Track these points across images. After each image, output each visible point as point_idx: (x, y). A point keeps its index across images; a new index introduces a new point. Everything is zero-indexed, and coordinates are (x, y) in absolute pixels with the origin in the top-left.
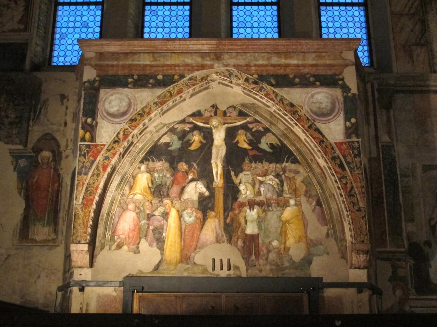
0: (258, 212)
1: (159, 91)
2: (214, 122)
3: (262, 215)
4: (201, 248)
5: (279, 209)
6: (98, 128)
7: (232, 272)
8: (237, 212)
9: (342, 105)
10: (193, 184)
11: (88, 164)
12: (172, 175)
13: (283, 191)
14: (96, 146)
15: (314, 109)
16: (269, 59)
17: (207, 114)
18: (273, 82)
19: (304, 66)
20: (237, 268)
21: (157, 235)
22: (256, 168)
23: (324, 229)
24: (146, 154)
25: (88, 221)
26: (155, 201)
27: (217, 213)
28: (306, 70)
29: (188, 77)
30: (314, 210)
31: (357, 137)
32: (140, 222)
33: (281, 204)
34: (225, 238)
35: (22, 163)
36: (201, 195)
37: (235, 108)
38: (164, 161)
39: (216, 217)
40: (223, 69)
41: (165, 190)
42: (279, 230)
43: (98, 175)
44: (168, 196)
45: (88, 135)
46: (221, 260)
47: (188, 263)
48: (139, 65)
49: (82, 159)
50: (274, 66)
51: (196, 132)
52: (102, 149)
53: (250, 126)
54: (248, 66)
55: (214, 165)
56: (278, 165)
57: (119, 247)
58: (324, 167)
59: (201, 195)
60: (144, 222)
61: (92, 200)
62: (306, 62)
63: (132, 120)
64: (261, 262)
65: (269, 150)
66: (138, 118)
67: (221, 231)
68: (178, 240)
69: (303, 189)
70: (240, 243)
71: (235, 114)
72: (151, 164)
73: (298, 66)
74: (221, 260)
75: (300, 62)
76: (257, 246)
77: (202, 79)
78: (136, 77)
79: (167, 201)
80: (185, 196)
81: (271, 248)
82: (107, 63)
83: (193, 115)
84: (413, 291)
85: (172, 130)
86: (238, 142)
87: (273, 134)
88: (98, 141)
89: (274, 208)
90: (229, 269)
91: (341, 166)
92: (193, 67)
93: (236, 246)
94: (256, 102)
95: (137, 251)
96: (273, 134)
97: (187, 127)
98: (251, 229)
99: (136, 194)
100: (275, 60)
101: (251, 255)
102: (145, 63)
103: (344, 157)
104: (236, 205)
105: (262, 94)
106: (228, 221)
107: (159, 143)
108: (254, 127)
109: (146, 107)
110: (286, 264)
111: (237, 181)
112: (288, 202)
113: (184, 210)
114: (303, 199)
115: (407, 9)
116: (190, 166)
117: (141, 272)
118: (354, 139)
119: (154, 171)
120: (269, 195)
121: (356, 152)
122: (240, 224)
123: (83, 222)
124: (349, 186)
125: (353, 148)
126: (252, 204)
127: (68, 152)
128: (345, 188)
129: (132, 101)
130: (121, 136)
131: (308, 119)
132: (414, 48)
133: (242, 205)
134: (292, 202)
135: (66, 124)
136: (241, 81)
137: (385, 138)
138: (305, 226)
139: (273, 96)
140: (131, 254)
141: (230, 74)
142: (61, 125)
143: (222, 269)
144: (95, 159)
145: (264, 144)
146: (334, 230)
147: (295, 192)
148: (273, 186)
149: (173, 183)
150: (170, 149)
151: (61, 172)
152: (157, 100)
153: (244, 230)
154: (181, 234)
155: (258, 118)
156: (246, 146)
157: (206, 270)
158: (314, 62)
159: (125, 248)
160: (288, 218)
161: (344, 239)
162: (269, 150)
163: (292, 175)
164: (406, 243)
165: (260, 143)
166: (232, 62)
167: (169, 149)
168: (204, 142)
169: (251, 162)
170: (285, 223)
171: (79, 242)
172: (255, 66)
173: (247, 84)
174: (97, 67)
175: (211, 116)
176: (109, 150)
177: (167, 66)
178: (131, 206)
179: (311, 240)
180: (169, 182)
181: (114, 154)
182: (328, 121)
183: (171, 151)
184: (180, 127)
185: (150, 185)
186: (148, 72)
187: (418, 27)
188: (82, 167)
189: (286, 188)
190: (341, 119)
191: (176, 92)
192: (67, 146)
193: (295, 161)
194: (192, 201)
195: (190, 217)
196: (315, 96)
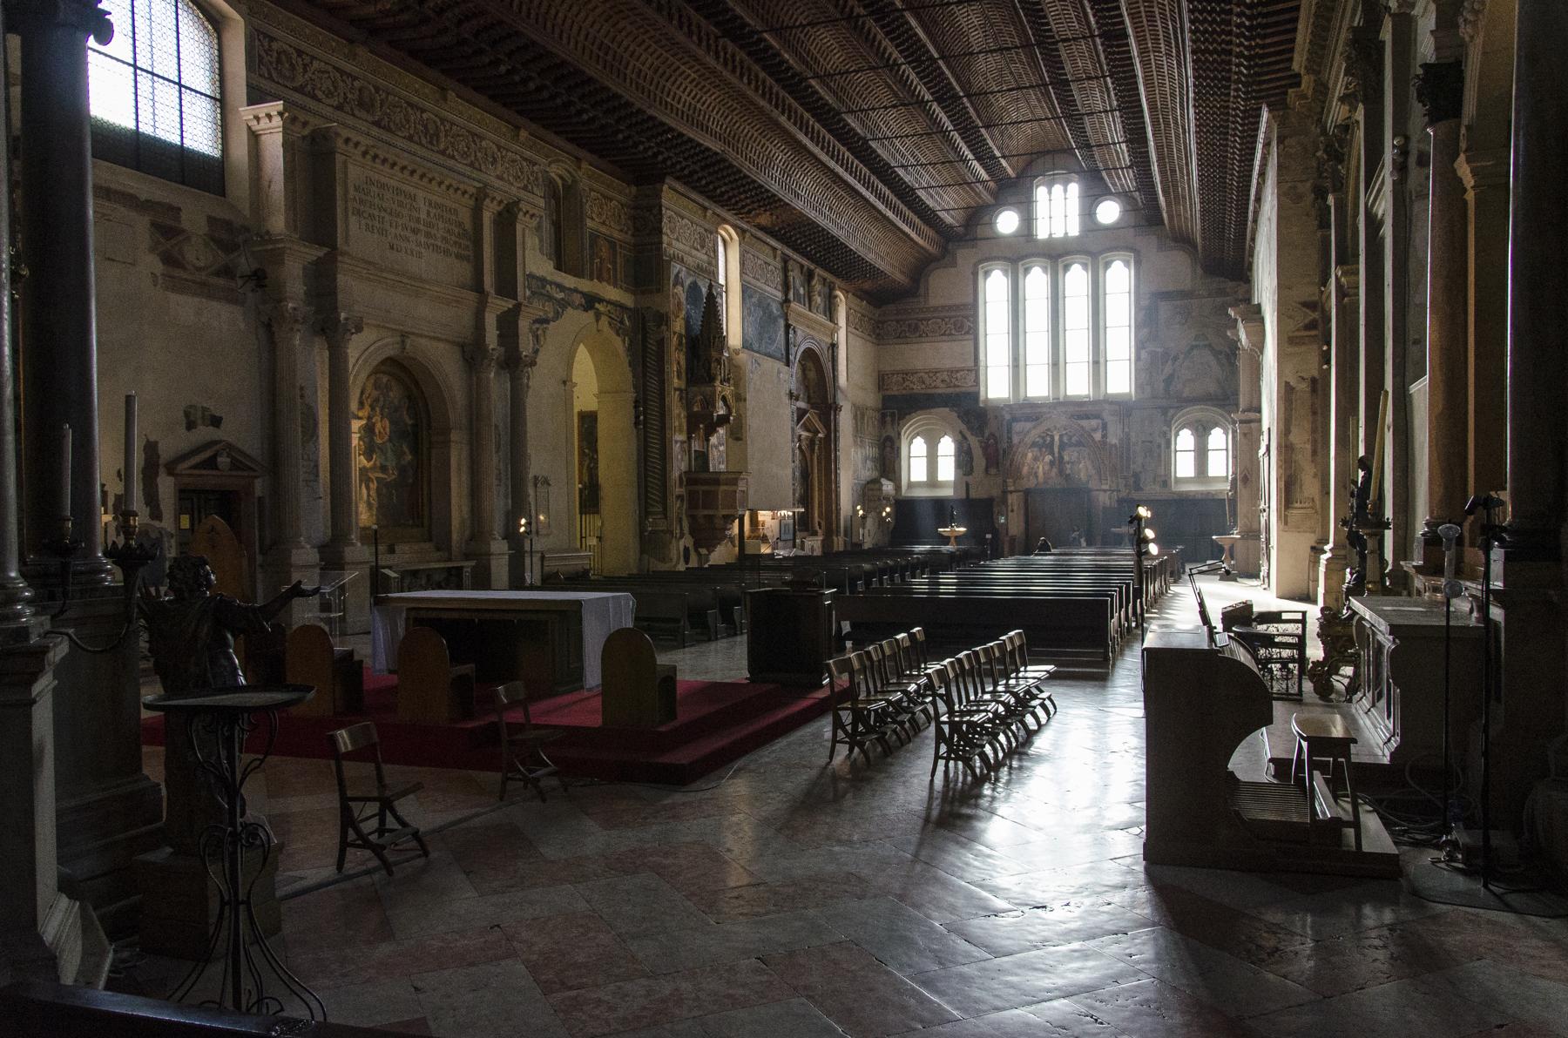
98: (1068, 472)
137: (1126, 430)
154: (1044, 474)
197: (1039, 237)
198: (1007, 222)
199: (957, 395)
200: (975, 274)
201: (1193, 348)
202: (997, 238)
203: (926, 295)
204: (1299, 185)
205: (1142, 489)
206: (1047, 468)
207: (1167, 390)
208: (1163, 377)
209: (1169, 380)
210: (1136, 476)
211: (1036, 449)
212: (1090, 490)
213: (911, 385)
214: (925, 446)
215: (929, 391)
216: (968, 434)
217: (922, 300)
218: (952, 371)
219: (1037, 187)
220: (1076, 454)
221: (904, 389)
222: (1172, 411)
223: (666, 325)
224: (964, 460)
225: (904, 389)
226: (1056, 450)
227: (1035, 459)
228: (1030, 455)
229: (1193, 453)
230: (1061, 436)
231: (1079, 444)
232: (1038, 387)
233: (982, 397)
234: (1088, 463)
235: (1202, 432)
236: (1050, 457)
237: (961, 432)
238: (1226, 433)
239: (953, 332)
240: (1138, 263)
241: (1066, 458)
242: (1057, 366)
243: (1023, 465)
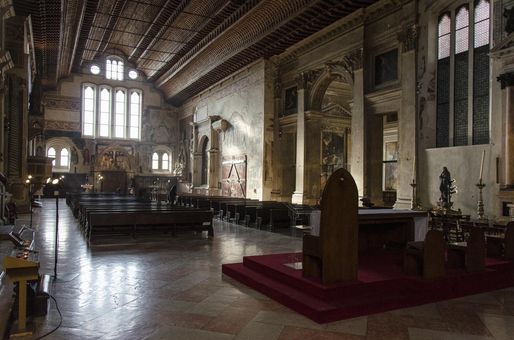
1: (107, 146)
35: (83, 153)
98: (118, 165)
100: (123, 143)
126: (119, 162)
137: (138, 151)
145: (121, 154)
174: (97, 142)
193: (125, 156)
197: (107, 78)
198: (95, 70)
199: (72, 132)
200: (81, 87)
201: (160, 126)
202: (92, 74)
203: (60, 91)
204: (270, 83)
205: (142, 173)
206: (110, 163)
207: (151, 139)
208: (150, 135)
209: (152, 136)
210: (141, 168)
212: (126, 172)
213: (51, 126)
214: (55, 152)
215: (59, 130)
216: (76, 148)
217: (57, 92)
218: (70, 123)
219: (107, 59)
220: (121, 159)
221: (48, 127)
222: (153, 146)
223: (25, 84)
224: (74, 158)
225: (48, 127)
226: (114, 157)
227: (106, 160)
228: (104, 158)
229: (158, 161)
230: (116, 152)
231: (123, 155)
232: (104, 133)
233: (82, 135)
234: (126, 162)
235: (161, 155)
236: (112, 159)
237: (73, 147)
238: (168, 155)
239: (71, 107)
240: (143, 95)
241: (118, 160)
242: (113, 126)
243: (101, 162)
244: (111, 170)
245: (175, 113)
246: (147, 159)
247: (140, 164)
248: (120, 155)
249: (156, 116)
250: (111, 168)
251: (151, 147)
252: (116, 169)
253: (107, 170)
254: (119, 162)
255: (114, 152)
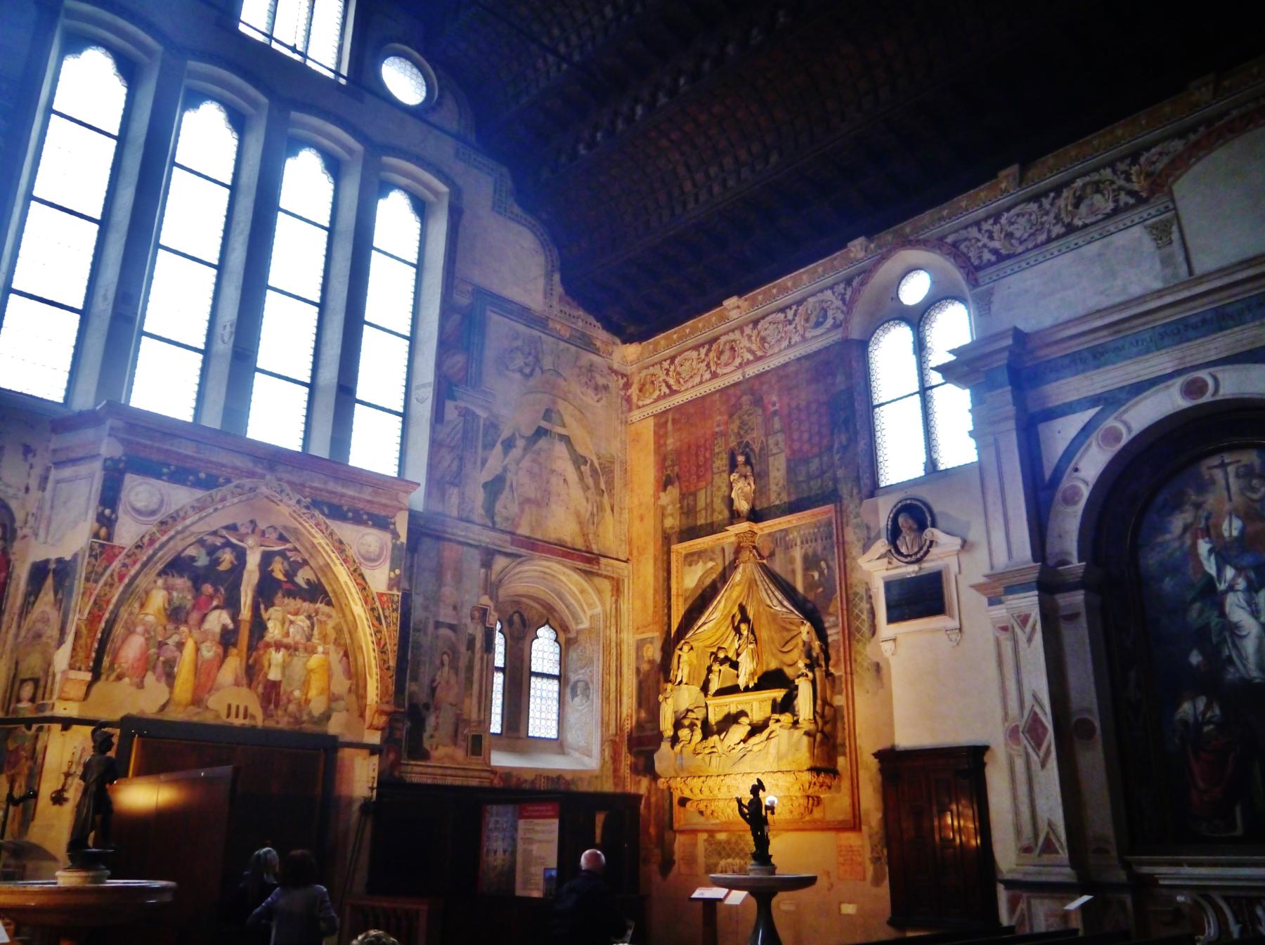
0: (284, 656)
1: (199, 493)
2: (250, 541)
3: (288, 659)
4: (218, 690)
5: (306, 655)
6: (118, 524)
7: (247, 722)
8: (261, 652)
9: (389, 553)
10: (216, 613)
11: (100, 570)
12: (194, 598)
13: (312, 635)
14: (113, 547)
15: (362, 551)
16: (325, 483)
17: (243, 530)
18: (326, 511)
19: (360, 499)
20: (253, 717)
21: (168, 669)
22: (288, 604)
23: (347, 683)
24: (165, 567)
25: (92, 643)
26: (170, 627)
27: (240, 651)
28: (361, 505)
29: (235, 482)
30: (340, 661)
31: (398, 590)
32: (148, 649)
33: (309, 649)
34: (245, 681)
36: (224, 628)
37: (275, 529)
38: (186, 579)
39: (238, 655)
40: (275, 483)
41: (183, 615)
42: (303, 678)
43: (112, 585)
44: (186, 622)
45: (103, 532)
46: (238, 707)
47: (199, 707)
48: (179, 454)
49: (93, 560)
50: (331, 492)
51: (228, 550)
52: (120, 553)
53: (289, 554)
54: (303, 485)
55: (243, 594)
56: (312, 605)
57: (119, 678)
58: (359, 616)
59: (224, 628)
60: (153, 651)
61: (100, 617)
62: (362, 496)
63: (162, 523)
64: (280, 712)
65: (305, 586)
66: (170, 521)
67: (241, 672)
68: (191, 678)
69: (332, 635)
70: (260, 689)
71: (274, 536)
72: (171, 580)
73: (353, 498)
74: (238, 707)
75: (356, 495)
76: (278, 694)
77: (251, 489)
78: (173, 468)
79: (183, 629)
80: (207, 626)
81: (292, 698)
82: (138, 440)
83: (227, 528)
84: (405, 755)
85: (201, 542)
86: (272, 571)
87: (312, 568)
88: (117, 541)
89: (301, 654)
90: (245, 717)
91: (378, 619)
92: (242, 472)
93: (256, 693)
94: (300, 526)
95: (140, 686)
96: (312, 568)
97: (219, 542)
98: (274, 675)
99: (147, 614)
101: (269, 702)
102: (186, 452)
103: (383, 609)
104: (261, 645)
105: (312, 522)
106: (251, 661)
107: (183, 555)
108: (294, 557)
109: (181, 509)
110: (305, 718)
111: (265, 616)
112: (316, 648)
113: (203, 642)
114: (331, 647)
115: (448, 440)
116: (216, 590)
117: (142, 711)
118: (395, 592)
119: (172, 589)
120: (298, 638)
121: (394, 606)
122: (263, 667)
123: (86, 646)
124: (383, 643)
125: (393, 602)
126: (278, 646)
127: (26, 531)
128: (378, 643)
129: (165, 499)
130: (146, 540)
131: (354, 561)
132: (447, 486)
133: (268, 645)
134: (320, 649)
135: (27, 489)
136: (293, 502)
138: (330, 677)
139: (323, 527)
140: (133, 689)
141: (282, 491)
142: (19, 490)
143: (237, 716)
144: (110, 563)
145: (301, 578)
146: (357, 685)
147: (324, 638)
148: (303, 628)
149: (194, 607)
150: (195, 564)
151: (12, 557)
152: (196, 504)
153: (266, 674)
154: (196, 669)
155: (299, 547)
156: (280, 576)
157: (218, 716)
158: (369, 498)
159: (126, 680)
160: (314, 667)
161: (364, 697)
162: (305, 586)
163: (324, 618)
164: (406, 705)
165: (295, 575)
166: (286, 476)
167: (195, 564)
168: (236, 563)
169: (284, 596)
170: (310, 671)
171: (80, 669)
172: (311, 487)
173: (297, 506)
175: (247, 534)
176: (128, 556)
177: (212, 462)
178: (140, 629)
179: (334, 694)
180: (189, 605)
181: (135, 563)
182: (373, 568)
183: (196, 567)
184: (210, 540)
185: (166, 606)
186: (188, 465)
187: (456, 464)
188: (92, 572)
189: (316, 632)
190: (387, 565)
191: (218, 498)
192: (26, 522)
193: (329, 603)
194: (214, 634)
195: (209, 651)
196: (366, 537)
205: (425, 756)
207: (490, 511)
208: (485, 476)
211: (181, 582)
220: (302, 621)
222: (500, 563)
226: (246, 597)
227: (175, 615)
230: (267, 558)
241: (274, 631)
244: (208, 718)
245: (616, 372)
246: (463, 648)
247: (411, 687)
248: (294, 592)
249: (519, 361)
250: (213, 701)
251: (487, 565)
252: (256, 709)
253: (176, 715)
254: (278, 646)
255: (253, 560)
